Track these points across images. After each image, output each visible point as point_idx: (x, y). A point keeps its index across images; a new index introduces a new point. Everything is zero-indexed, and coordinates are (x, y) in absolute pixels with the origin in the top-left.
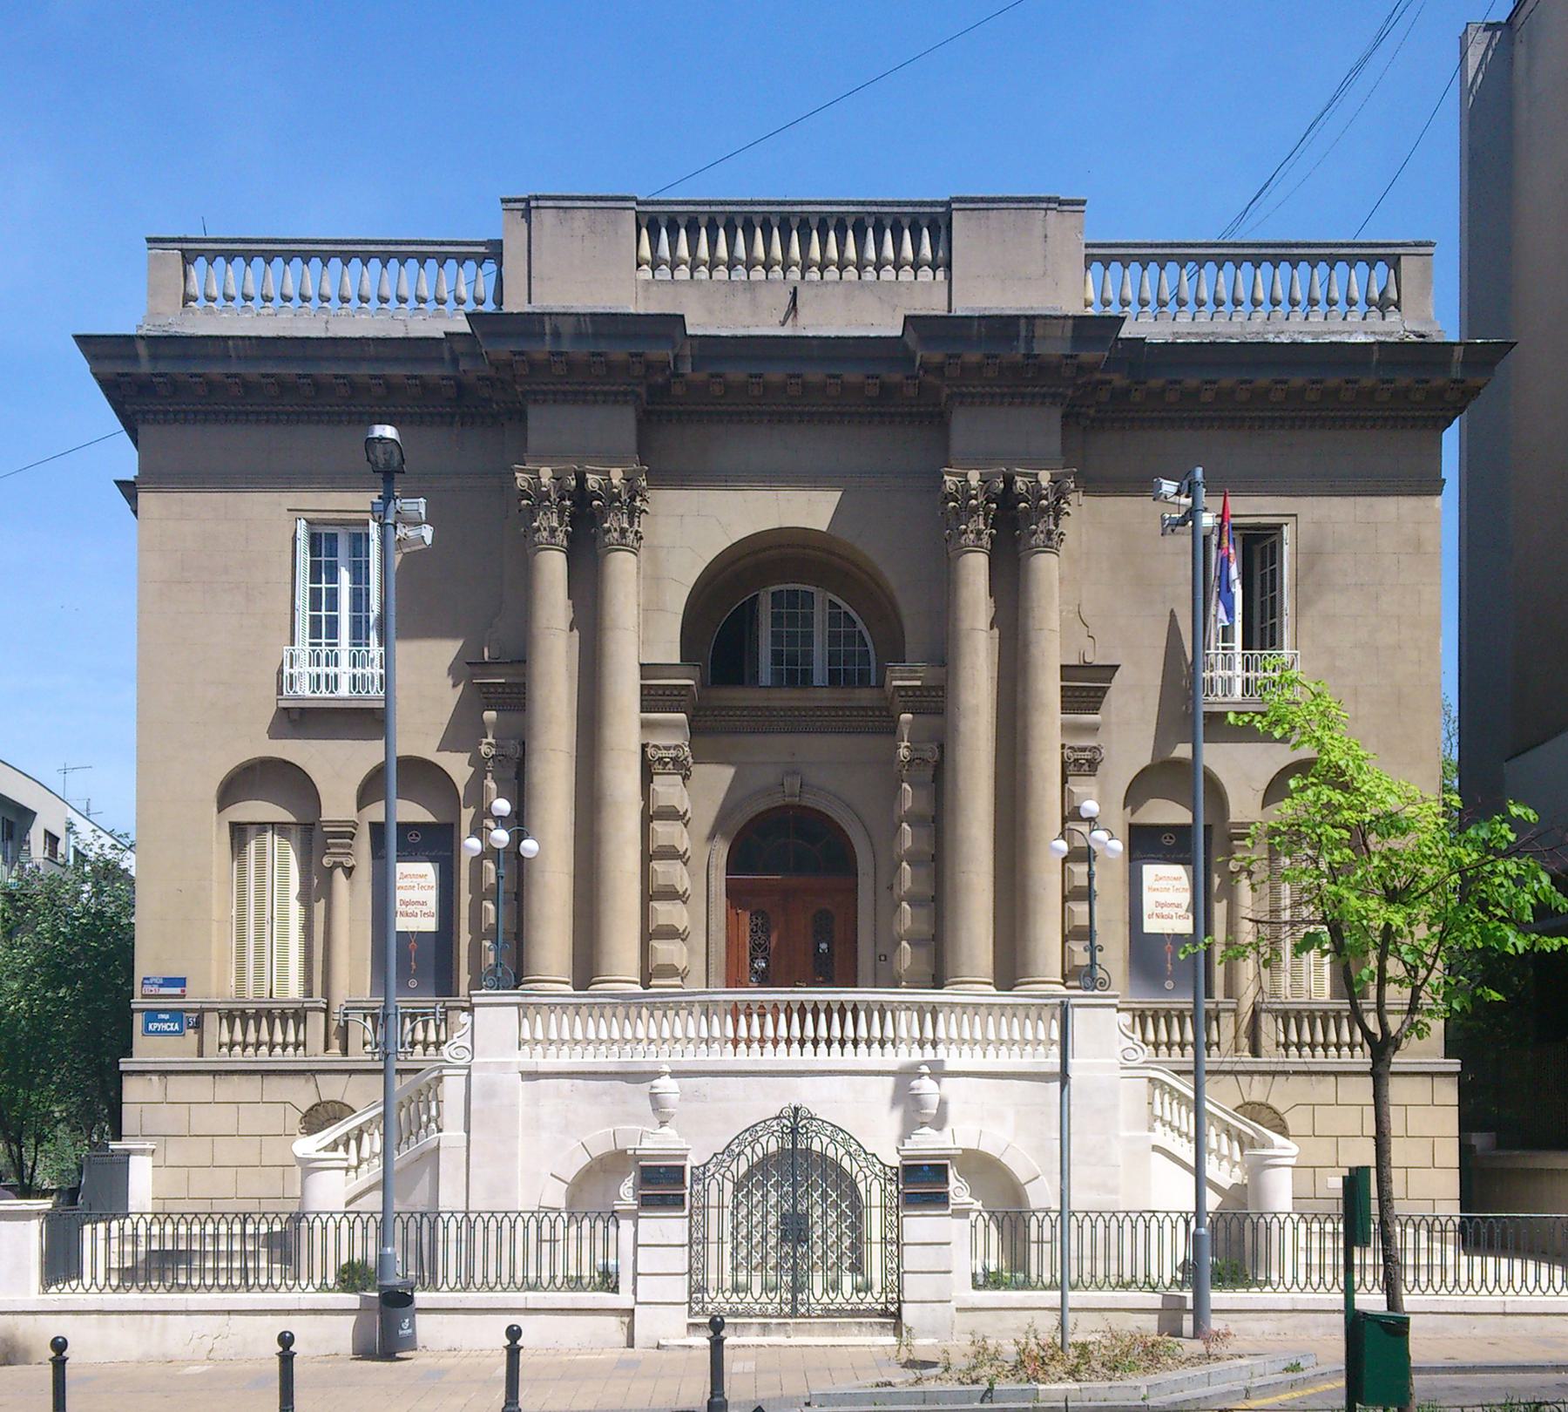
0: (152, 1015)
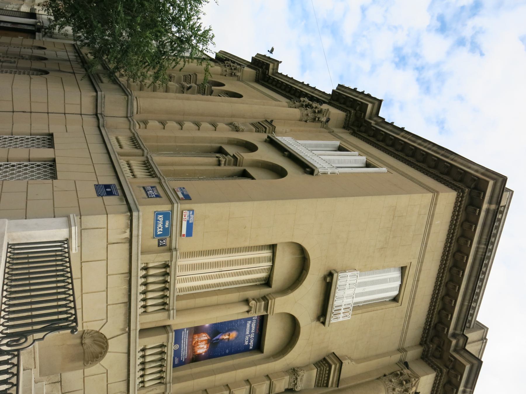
0: (167, 216)
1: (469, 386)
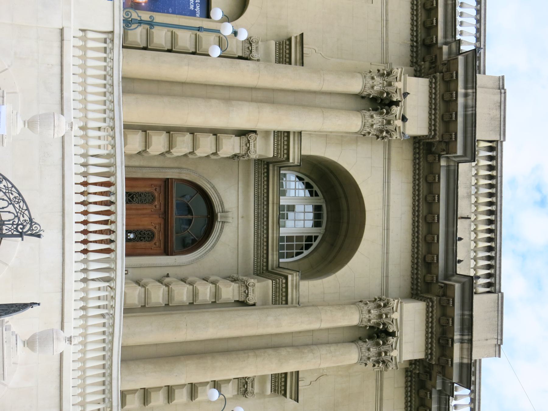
1: (470, 85)
